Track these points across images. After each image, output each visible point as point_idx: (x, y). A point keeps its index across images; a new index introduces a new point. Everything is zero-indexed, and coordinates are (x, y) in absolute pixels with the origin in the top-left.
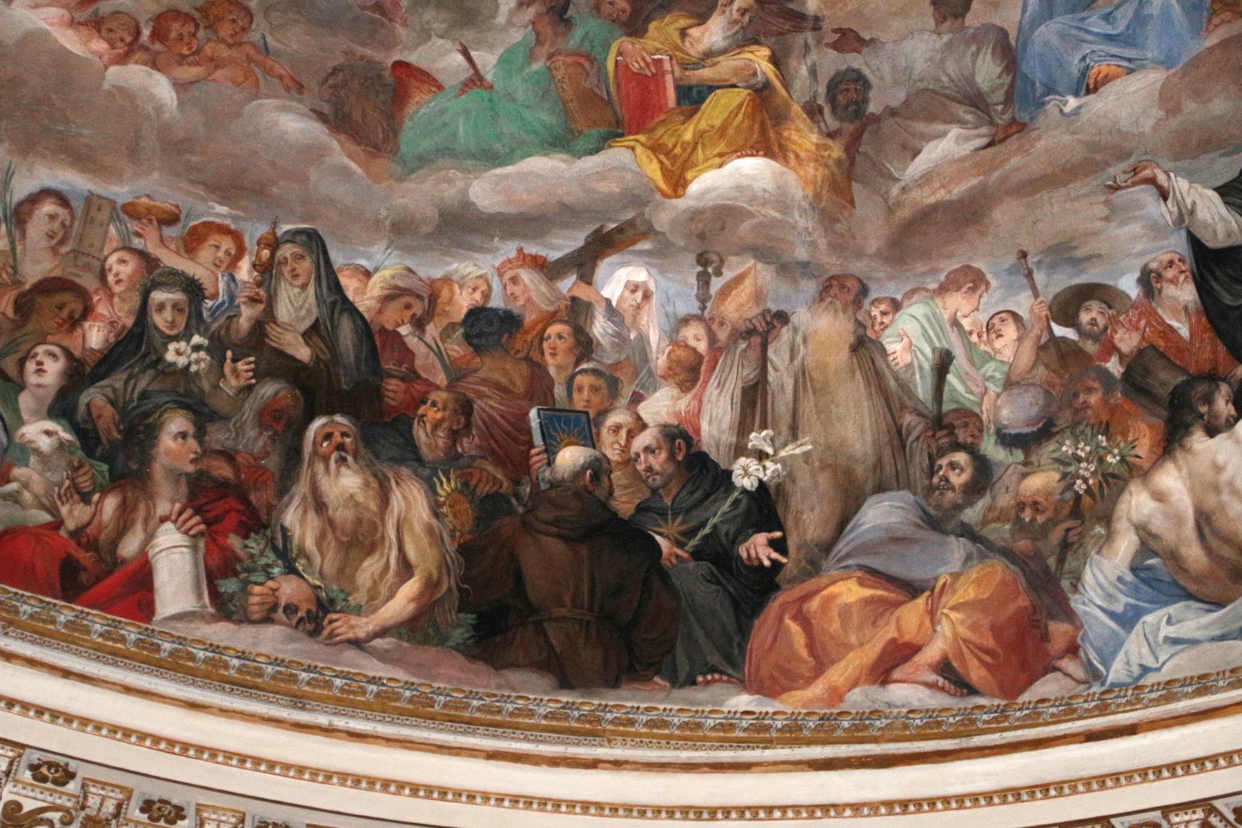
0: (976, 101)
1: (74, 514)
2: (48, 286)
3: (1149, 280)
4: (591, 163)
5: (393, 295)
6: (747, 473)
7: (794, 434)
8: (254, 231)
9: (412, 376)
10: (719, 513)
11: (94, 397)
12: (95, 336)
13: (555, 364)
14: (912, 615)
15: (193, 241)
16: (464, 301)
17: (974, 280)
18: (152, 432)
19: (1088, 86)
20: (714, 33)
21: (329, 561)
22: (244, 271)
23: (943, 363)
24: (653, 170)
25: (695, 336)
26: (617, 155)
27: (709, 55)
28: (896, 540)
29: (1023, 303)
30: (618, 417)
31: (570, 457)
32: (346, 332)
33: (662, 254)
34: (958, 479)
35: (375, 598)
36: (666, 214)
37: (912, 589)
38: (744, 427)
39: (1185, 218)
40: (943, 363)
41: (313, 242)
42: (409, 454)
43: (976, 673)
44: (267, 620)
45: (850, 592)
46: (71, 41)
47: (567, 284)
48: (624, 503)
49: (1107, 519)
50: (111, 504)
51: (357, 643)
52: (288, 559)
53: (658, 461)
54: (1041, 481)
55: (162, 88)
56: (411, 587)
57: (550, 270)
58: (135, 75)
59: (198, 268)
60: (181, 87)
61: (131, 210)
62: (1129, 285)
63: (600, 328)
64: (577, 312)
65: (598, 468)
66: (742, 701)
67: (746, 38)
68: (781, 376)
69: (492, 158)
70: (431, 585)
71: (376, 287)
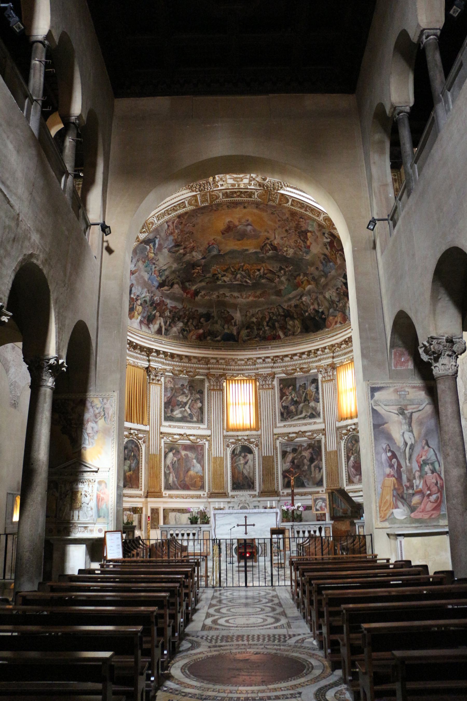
0: (323, 276)
1: (272, 333)
2: (262, 317)
3: (341, 286)
4: (297, 291)
5: (288, 307)
6: (320, 310)
7: (322, 306)
8: (275, 306)
9: (292, 312)
10: (320, 314)
11: (270, 324)
12: (267, 319)
13: (302, 307)
14: (336, 319)
15: (271, 309)
16: (293, 305)
17: (329, 289)
18: (275, 325)
19: (330, 272)
20: (301, 277)
21: (292, 329)
22: (276, 310)
23: (331, 297)
24: (302, 289)
25: (312, 301)
26: (299, 289)
27: (302, 279)
28: (333, 312)
29: (334, 290)
30: (309, 309)
31: (307, 314)
32: (286, 311)
33: (306, 295)
34: (335, 306)
35: (297, 331)
36: (305, 292)
37: (336, 316)
38: (319, 307)
39: (341, 281)
40: (331, 297)
41: (280, 305)
42: (295, 319)
43: (342, 322)
44: (290, 335)
45: (331, 318)
46: (254, 299)
47: (300, 301)
48: (312, 316)
49: (346, 306)
50: (274, 331)
51: (297, 335)
52: (289, 330)
53: (313, 312)
54: (341, 305)
55: (263, 299)
56: (299, 329)
57: (298, 300)
58: (260, 299)
59: (272, 311)
60: (264, 298)
61: (265, 309)
62: (340, 287)
63: (304, 303)
64: (302, 302)
65: (309, 314)
66: (327, 330)
67: (304, 276)
68: (320, 302)
69: (290, 293)
70: (301, 328)
71: (286, 307)
